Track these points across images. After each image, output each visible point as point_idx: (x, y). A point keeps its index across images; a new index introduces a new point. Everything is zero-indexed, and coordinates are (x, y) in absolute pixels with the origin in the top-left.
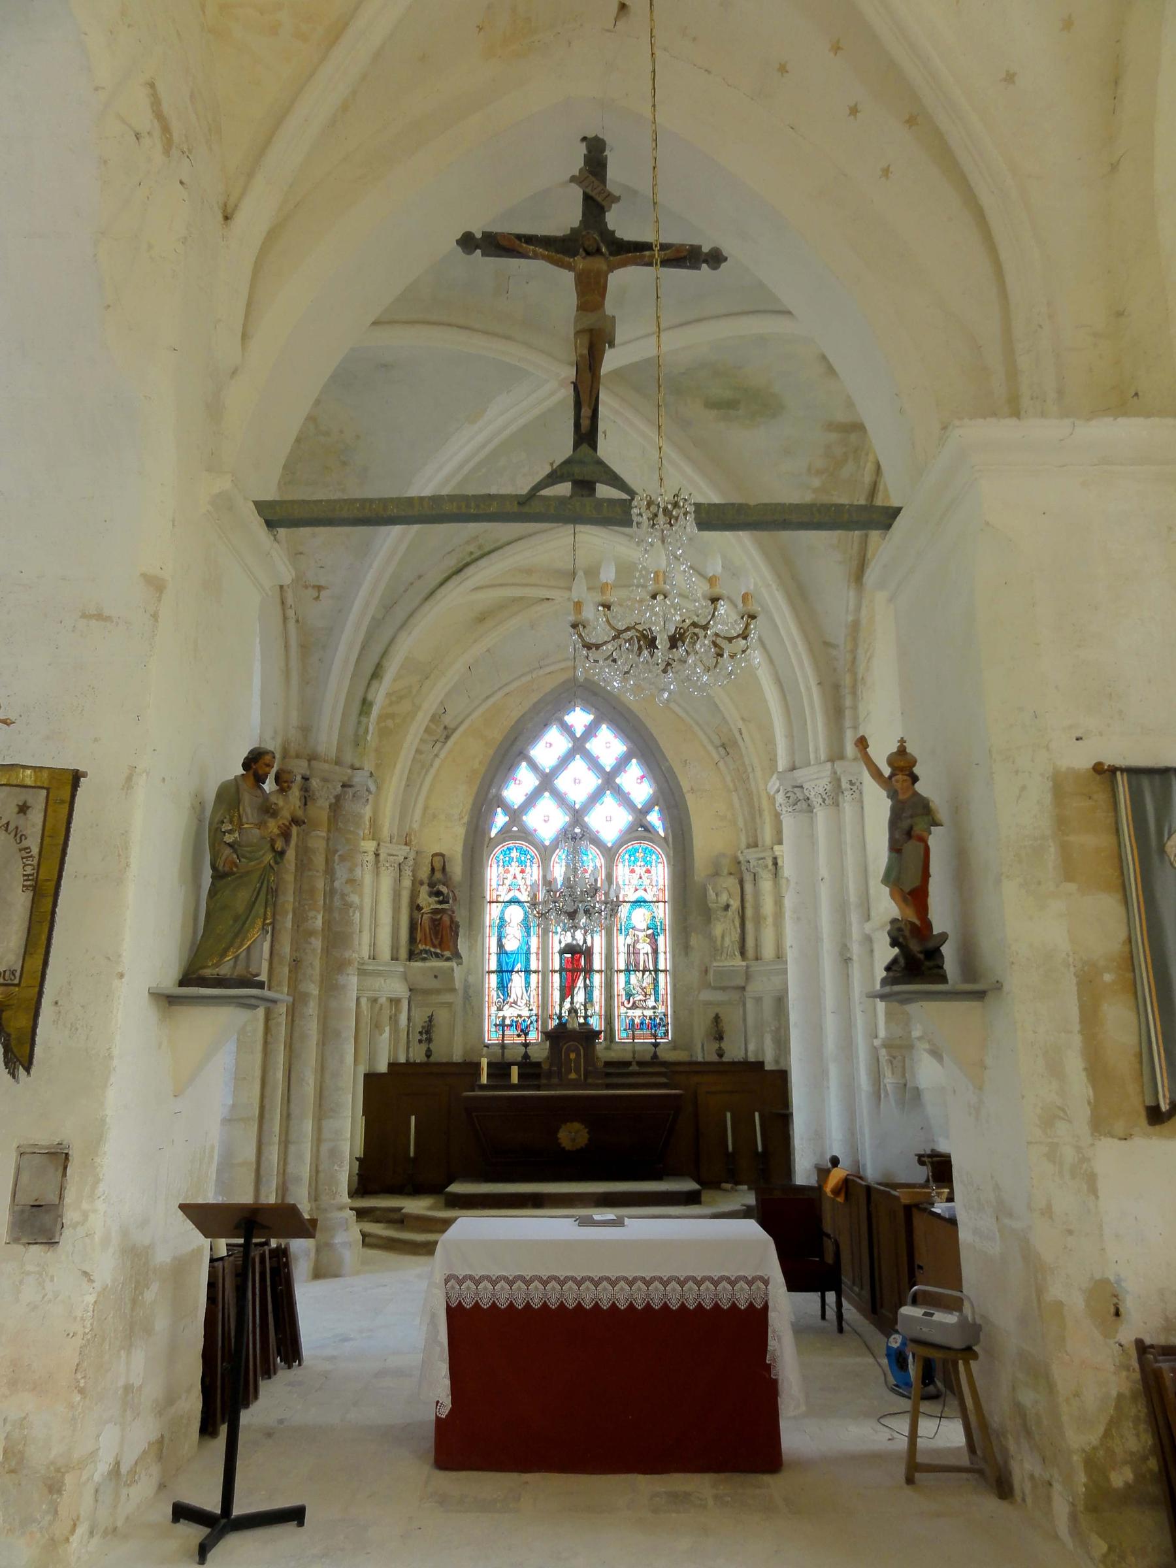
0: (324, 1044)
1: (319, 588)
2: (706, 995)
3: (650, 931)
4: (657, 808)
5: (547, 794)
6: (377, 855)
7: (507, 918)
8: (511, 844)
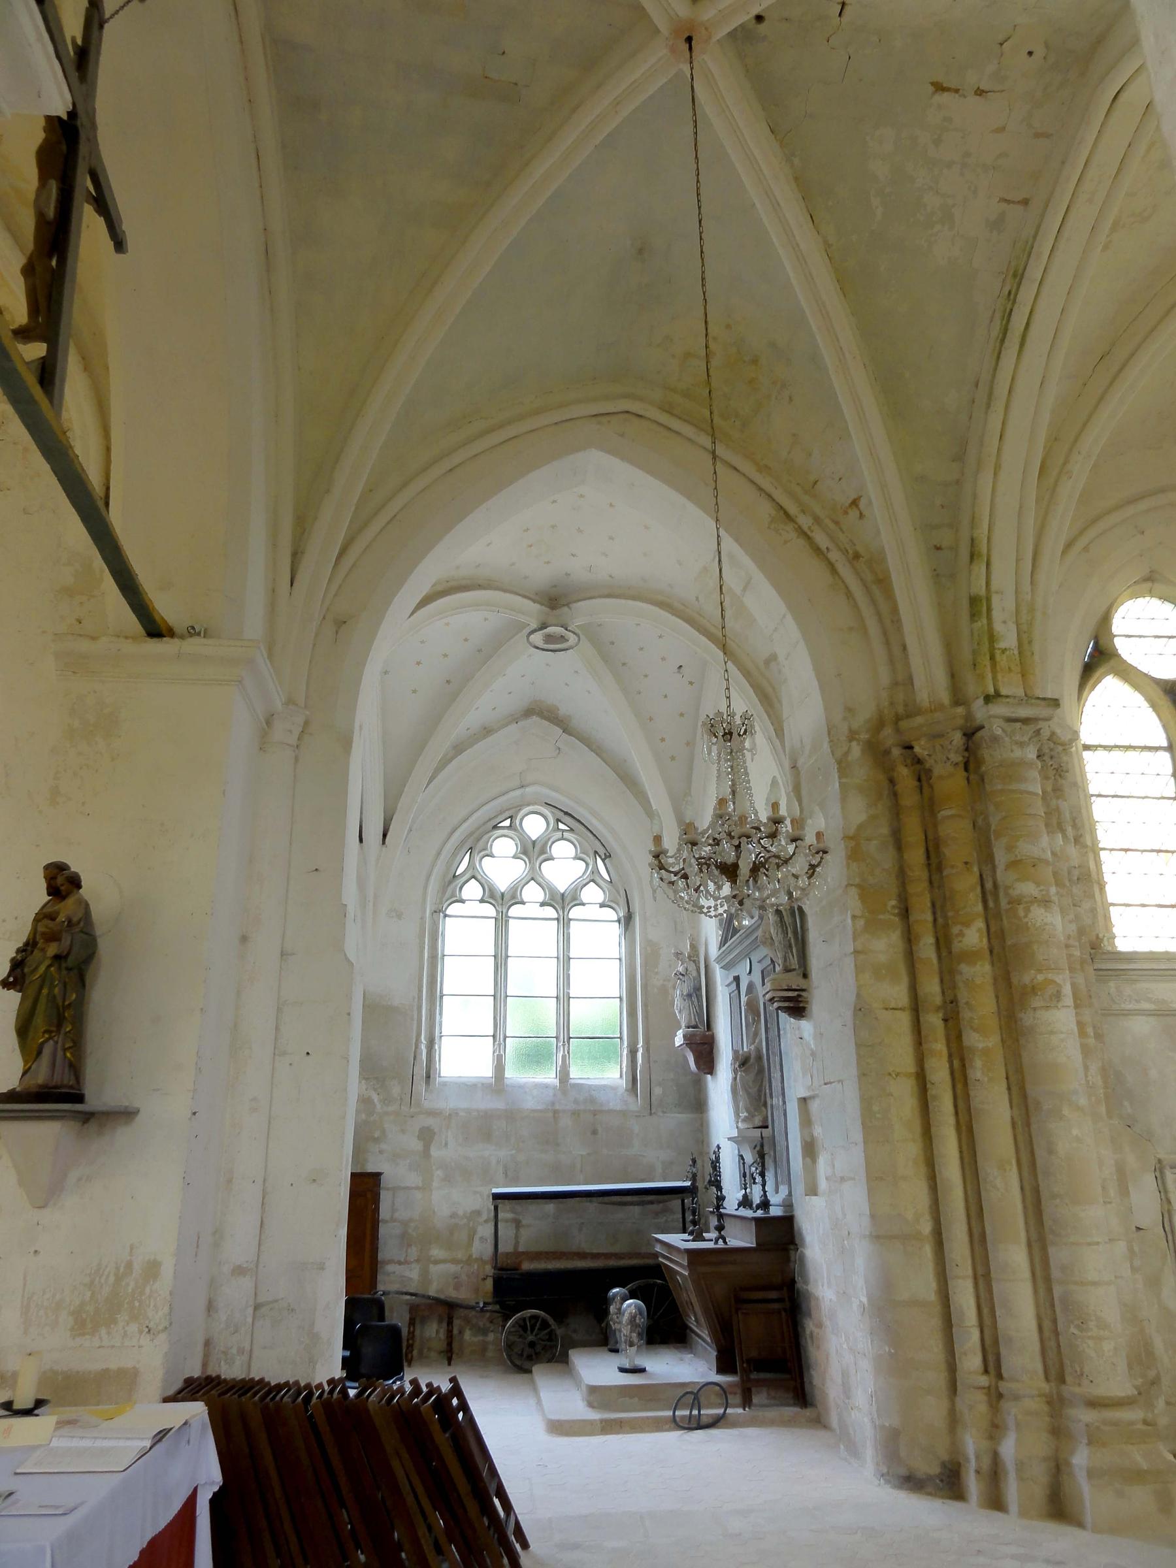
1: (855, 503)
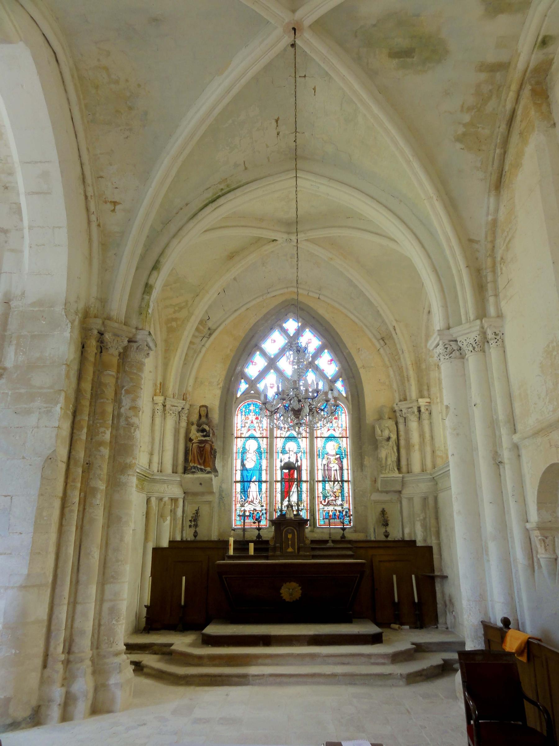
0: (108, 527)
1: (115, 203)
2: (375, 497)
3: (338, 456)
4: (341, 379)
5: (272, 371)
6: (164, 406)
7: (247, 447)
8: (249, 401)
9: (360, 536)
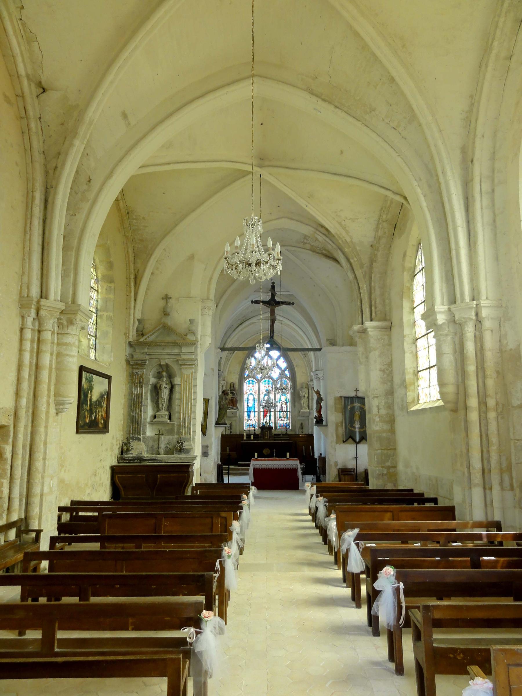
2: (299, 418)
9: (293, 433)
